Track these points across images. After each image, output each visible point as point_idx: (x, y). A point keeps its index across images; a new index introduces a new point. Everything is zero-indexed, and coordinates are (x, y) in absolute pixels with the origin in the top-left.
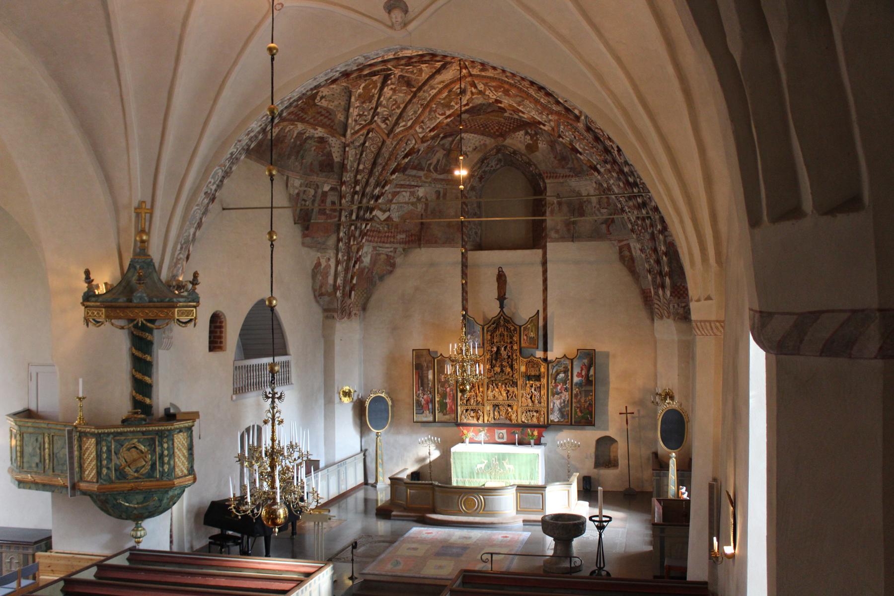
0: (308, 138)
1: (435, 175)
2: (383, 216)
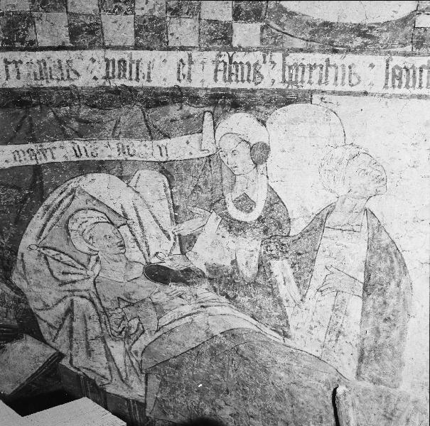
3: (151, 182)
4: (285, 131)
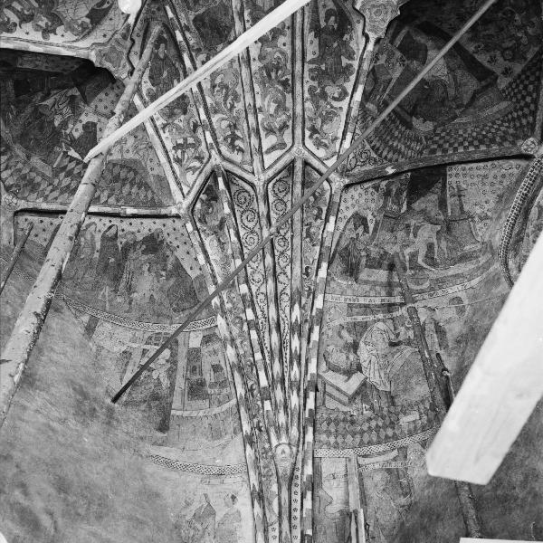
1: (434, 273)
2: (354, 383)
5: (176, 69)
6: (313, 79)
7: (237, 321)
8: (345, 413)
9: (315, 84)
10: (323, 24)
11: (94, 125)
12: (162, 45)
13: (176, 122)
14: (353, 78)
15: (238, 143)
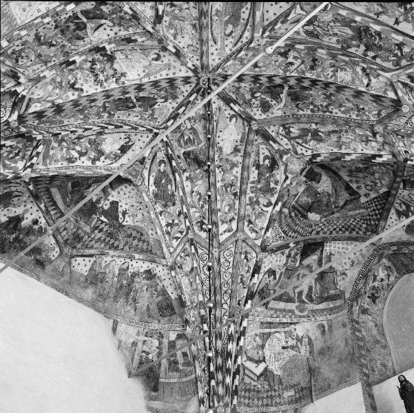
0: (134, 275)
1: (310, 306)
2: (259, 370)
3: (283, 334)
4: (297, 327)
5: (170, 179)
6: (252, 192)
7: (197, 328)
8: (255, 386)
9: (253, 195)
10: (261, 163)
11: (117, 203)
12: (163, 165)
13: (168, 210)
14: (276, 196)
15: (204, 226)
